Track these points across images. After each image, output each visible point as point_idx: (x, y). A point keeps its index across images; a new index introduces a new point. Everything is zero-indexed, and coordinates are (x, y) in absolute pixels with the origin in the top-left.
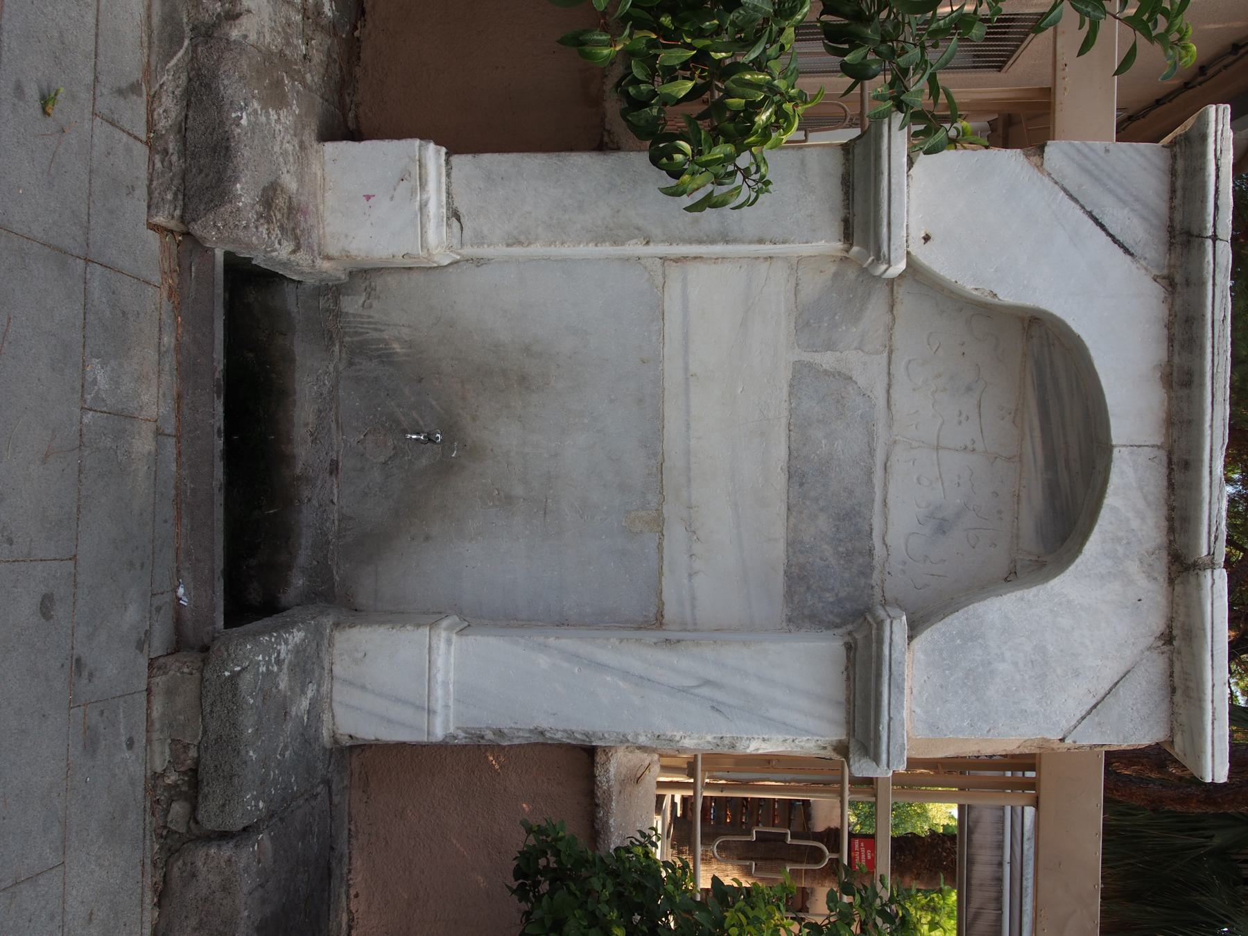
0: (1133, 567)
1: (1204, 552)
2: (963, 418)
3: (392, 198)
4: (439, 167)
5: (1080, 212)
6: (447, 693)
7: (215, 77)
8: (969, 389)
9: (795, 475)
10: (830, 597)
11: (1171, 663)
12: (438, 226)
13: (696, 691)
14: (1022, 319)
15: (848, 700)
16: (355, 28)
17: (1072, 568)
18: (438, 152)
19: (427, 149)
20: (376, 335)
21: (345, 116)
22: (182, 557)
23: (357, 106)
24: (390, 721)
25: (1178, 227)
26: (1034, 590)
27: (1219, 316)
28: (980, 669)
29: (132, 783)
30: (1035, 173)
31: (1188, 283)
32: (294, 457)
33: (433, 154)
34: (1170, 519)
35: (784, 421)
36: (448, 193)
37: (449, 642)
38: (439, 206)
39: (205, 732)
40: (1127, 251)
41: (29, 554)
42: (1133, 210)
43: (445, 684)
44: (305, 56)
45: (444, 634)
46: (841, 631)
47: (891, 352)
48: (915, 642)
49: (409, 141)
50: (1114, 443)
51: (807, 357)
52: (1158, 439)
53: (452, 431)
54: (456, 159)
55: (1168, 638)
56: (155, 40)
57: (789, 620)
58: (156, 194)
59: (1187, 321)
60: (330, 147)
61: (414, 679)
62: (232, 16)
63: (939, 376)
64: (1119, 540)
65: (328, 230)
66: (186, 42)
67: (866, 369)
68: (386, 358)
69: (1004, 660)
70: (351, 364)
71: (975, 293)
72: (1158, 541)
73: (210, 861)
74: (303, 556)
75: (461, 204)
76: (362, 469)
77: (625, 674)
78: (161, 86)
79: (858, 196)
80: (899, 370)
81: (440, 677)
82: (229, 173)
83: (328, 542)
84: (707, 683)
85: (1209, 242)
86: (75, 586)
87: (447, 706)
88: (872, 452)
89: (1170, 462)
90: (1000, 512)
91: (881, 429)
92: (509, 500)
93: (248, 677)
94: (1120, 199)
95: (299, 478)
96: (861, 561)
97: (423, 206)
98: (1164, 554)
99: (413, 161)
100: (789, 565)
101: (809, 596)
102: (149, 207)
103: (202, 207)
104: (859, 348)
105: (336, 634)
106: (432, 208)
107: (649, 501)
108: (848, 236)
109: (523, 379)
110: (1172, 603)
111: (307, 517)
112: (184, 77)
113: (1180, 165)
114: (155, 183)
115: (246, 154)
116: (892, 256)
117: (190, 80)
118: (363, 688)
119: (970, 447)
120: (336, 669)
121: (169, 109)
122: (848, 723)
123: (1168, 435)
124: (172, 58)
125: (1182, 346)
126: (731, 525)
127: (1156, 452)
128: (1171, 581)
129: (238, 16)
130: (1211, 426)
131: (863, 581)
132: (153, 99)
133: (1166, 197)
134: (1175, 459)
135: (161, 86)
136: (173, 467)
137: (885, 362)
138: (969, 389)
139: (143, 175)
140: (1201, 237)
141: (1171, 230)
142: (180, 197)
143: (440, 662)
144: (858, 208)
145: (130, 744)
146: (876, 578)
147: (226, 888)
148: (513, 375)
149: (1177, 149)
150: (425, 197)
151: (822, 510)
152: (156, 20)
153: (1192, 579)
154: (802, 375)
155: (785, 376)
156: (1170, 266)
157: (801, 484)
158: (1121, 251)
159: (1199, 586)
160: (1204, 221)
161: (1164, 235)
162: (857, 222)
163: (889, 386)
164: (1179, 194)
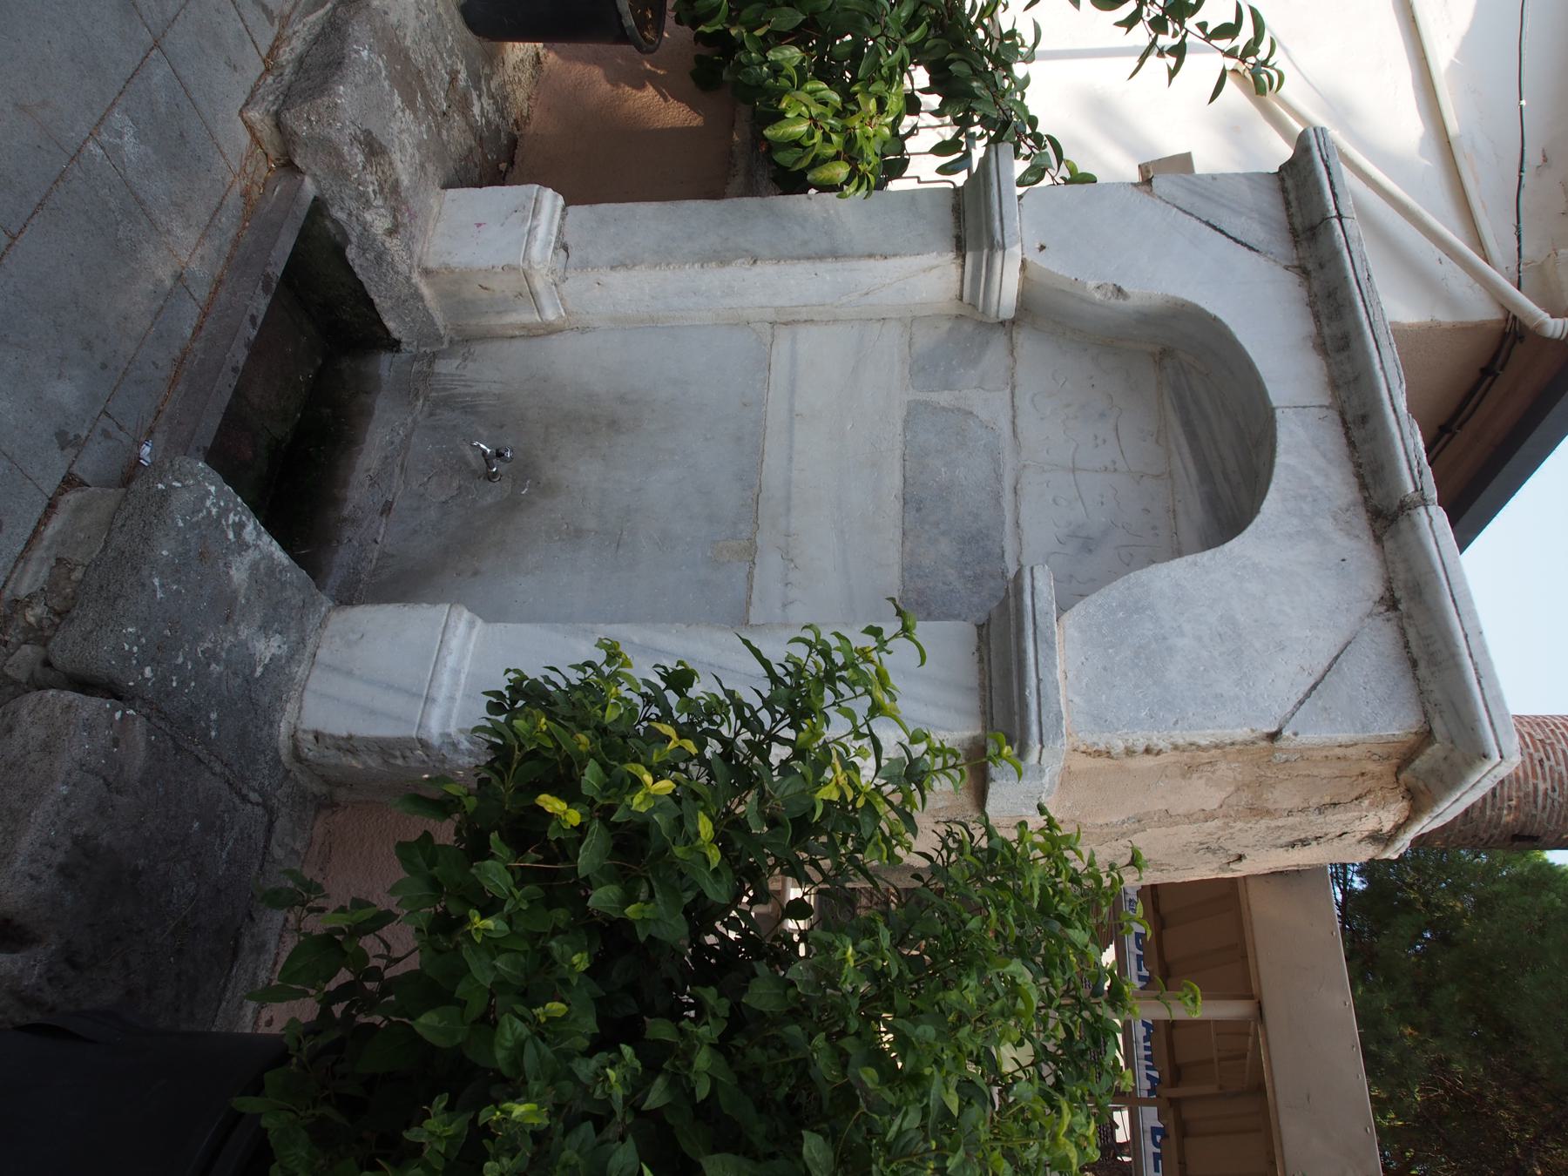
0: (1327, 525)
1: (1411, 489)
2: (1099, 441)
4: (554, 212)
6: (456, 683)
9: (911, 501)
11: (1403, 632)
14: (1152, 354)
15: (982, 686)
24: (372, 712)
26: (1209, 553)
28: (1154, 646)
31: (1321, 266)
33: (550, 200)
34: (1359, 476)
35: (898, 453)
37: (471, 625)
47: (1013, 388)
48: (1066, 616)
50: (1275, 404)
53: (526, 471)
55: (1390, 602)
63: (1068, 405)
67: (989, 405)
69: (1182, 634)
71: (1098, 296)
76: (418, 509)
79: (969, 217)
80: (1023, 403)
81: (451, 661)
85: (1335, 222)
87: (452, 698)
88: (999, 478)
89: (1344, 422)
92: (579, 533)
95: (345, 520)
96: (992, 584)
98: (1361, 511)
106: (541, 232)
108: (960, 247)
110: (1385, 562)
118: (350, 674)
120: (321, 653)
122: (984, 713)
123: (1333, 396)
125: (1330, 318)
127: (1325, 412)
128: (1378, 539)
130: (1383, 368)
133: (1282, 208)
134: (1349, 418)
138: (1102, 415)
140: (1326, 220)
141: (1293, 232)
143: (454, 643)
148: (603, 420)
151: (943, 534)
154: (914, 413)
156: (1299, 259)
157: (919, 510)
159: (1414, 527)
163: (1014, 417)
164: (1294, 204)
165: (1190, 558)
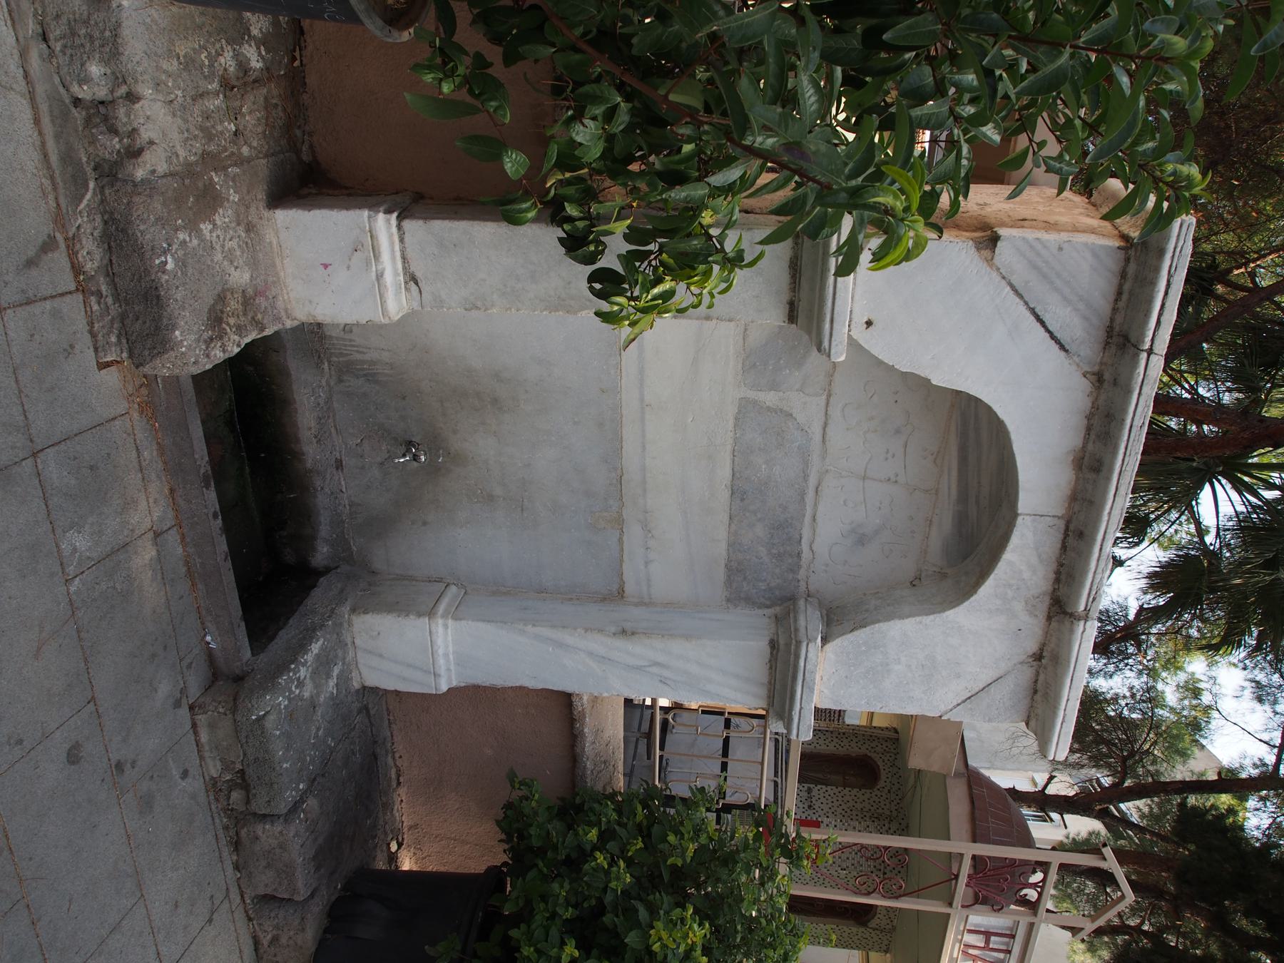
0: (1019, 607)
1: (1082, 608)
2: (889, 455)
3: (348, 268)
4: (391, 236)
5: (1022, 308)
6: (448, 661)
7: (129, 222)
8: (898, 431)
9: (738, 492)
10: (763, 586)
11: (1038, 674)
12: (398, 293)
13: (650, 669)
15: (770, 683)
16: (294, 59)
17: (966, 604)
18: (388, 221)
19: (376, 221)
20: (359, 357)
21: (298, 153)
22: (204, 613)
23: (310, 134)
24: (404, 679)
25: (1117, 329)
26: (932, 617)
27: (1138, 422)
29: (193, 797)
30: (984, 267)
32: (303, 454)
33: (384, 225)
34: (1058, 573)
35: (729, 448)
36: (404, 258)
37: (446, 626)
38: (396, 274)
39: (245, 755)
40: (1062, 347)
41: (43, 734)
42: (1076, 310)
43: (446, 655)
44: (236, 133)
45: (440, 621)
46: (768, 612)
47: (829, 396)
48: (829, 647)
49: (358, 212)
51: (752, 394)
52: (1060, 511)
53: (435, 443)
54: (407, 224)
55: (1038, 657)
56: (59, 180)
57: (728, 600)
58: (100, 337)
59: (1107, 416)
60: (285, 217)
61: (420, 649)
62: (134, 153)
63: (872, 418)
64: (1010, 586)
65: (292, 295)
66: (92, 185)
68: (371, 377)
70: (340, 381)
72: (1044, 589)
73: (268, 834)
74: (324, 530)
75: (418, 269)
76: (363, 468)
77: (591, 654)
78: (79, 228)
79: (805, 284)
80: (835, 412)
81: (441, 652)
82: (165, 321)
83: (343, 522)
84: (656, 664)
85: (1144, 355)
86: (99, 717)
87: (449, 670)
88: (806, 478)
90: (913, 532)
91: (815, 458)
92: (491, 498)
93: (272, 717)
94: (1065, 299)
95: (311, 471)
97: (380, 276)
99: (363, 230)
100: (729, 560)
101: (745, 584)
102: (96, 350)
103: (147, 353)
104: (801, 390)
105: (354, 617)
106: (388, 278)
107: (610, 503)
108: (792, 317)
109: (495, 401)
111: (322, 500)
112: (98, 219)
113: (1132, 268)
114: (96, 325)
115: (179, 296)
116: (833, 351)
117: (106, 223)
118: (381, 656)
119: (893, 479)
120: (357, 642)
121: (91, 255)
122: (769, 697)
123: (1070, 507)
124: (81, 201)
125: (1098, 436)
126: (681, 526)
127: (1056, 521)
128: (1049, 618)
129: (140, 152)
130: (1110, 514)
131: (791, 576)
132: (72, 244)
133: (1112, 298)
134: (1072, 527)
135: (79, 228)
136: (180, 550)
137: (823, 403)
138: (898, 431)
139: (82, 324)
140: (1137, 348)
141: (1110, 331)
142: (124, 341)
143: (440, 641)
144: (804, 293)
145: (185, 774)
146: (802, 574)
147: (282, 846)
148: (488, 396)
149: (1132, 252)
150: (380, 267)
151: (759, 520)
152: (54, 158)
153: (1067, 623)
154: (746, 409)
155: (731, 411)
156: (1101, 363)
158: (1056, 347)
159: (1072, 631)
160: (1143, 335)
161: (1102, 335)
162: (802, 307)
163: (826, 425)
164: (1125, 297)
165: (918, 619)
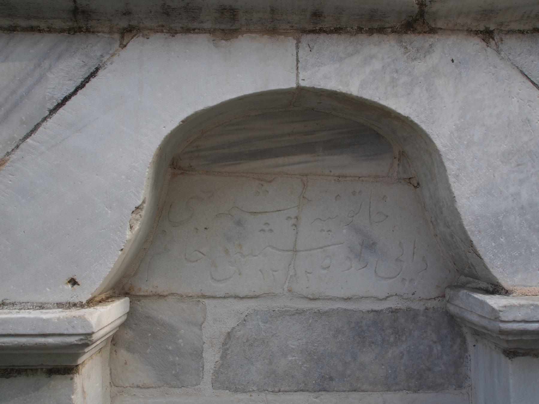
0: (420, 67)
8: (239, 223)
9: (323, 385)
10: (437, 349)
11: (511, 32)
14: (174, 175)
17: (423, 126)
25: (70, 24)
26: (447, 164)
28: (528, 217)
31: (127, 13)
34: (371, 32)
40: (93, 74)
42: (50, 68)
47: (204, 297)
48: (505, 282)
50: (294, 85)
51: (208, 377)
52: (291, 42)
55: (487, 35)
59: (168, 14)
63: (227, 251)
67: (220, 319)
69: (518, 194)
71: (137, 227)
72: (393, 43)
80: (222, 288)
88: (300, 312)
89: (313, 32)
96: (402, 320)
98: (407, 37)
100: (409, 389)
104: (200, 326)
110: (454, 30)
116: (81, 331)
119: (293, 221)
123: (286, 33)
125: (194, 19)
127: (304, 44)
128: (433, 31)
134: (310, 27)
138: (239, 223)
141: (73, 31)
146: (417, 306)
154: (224, 381)
156: (111, 32)
157: (331, 379)
161: (78, 38)
163: (236, 297)
164: (34, 23)
165: (452, 180)
